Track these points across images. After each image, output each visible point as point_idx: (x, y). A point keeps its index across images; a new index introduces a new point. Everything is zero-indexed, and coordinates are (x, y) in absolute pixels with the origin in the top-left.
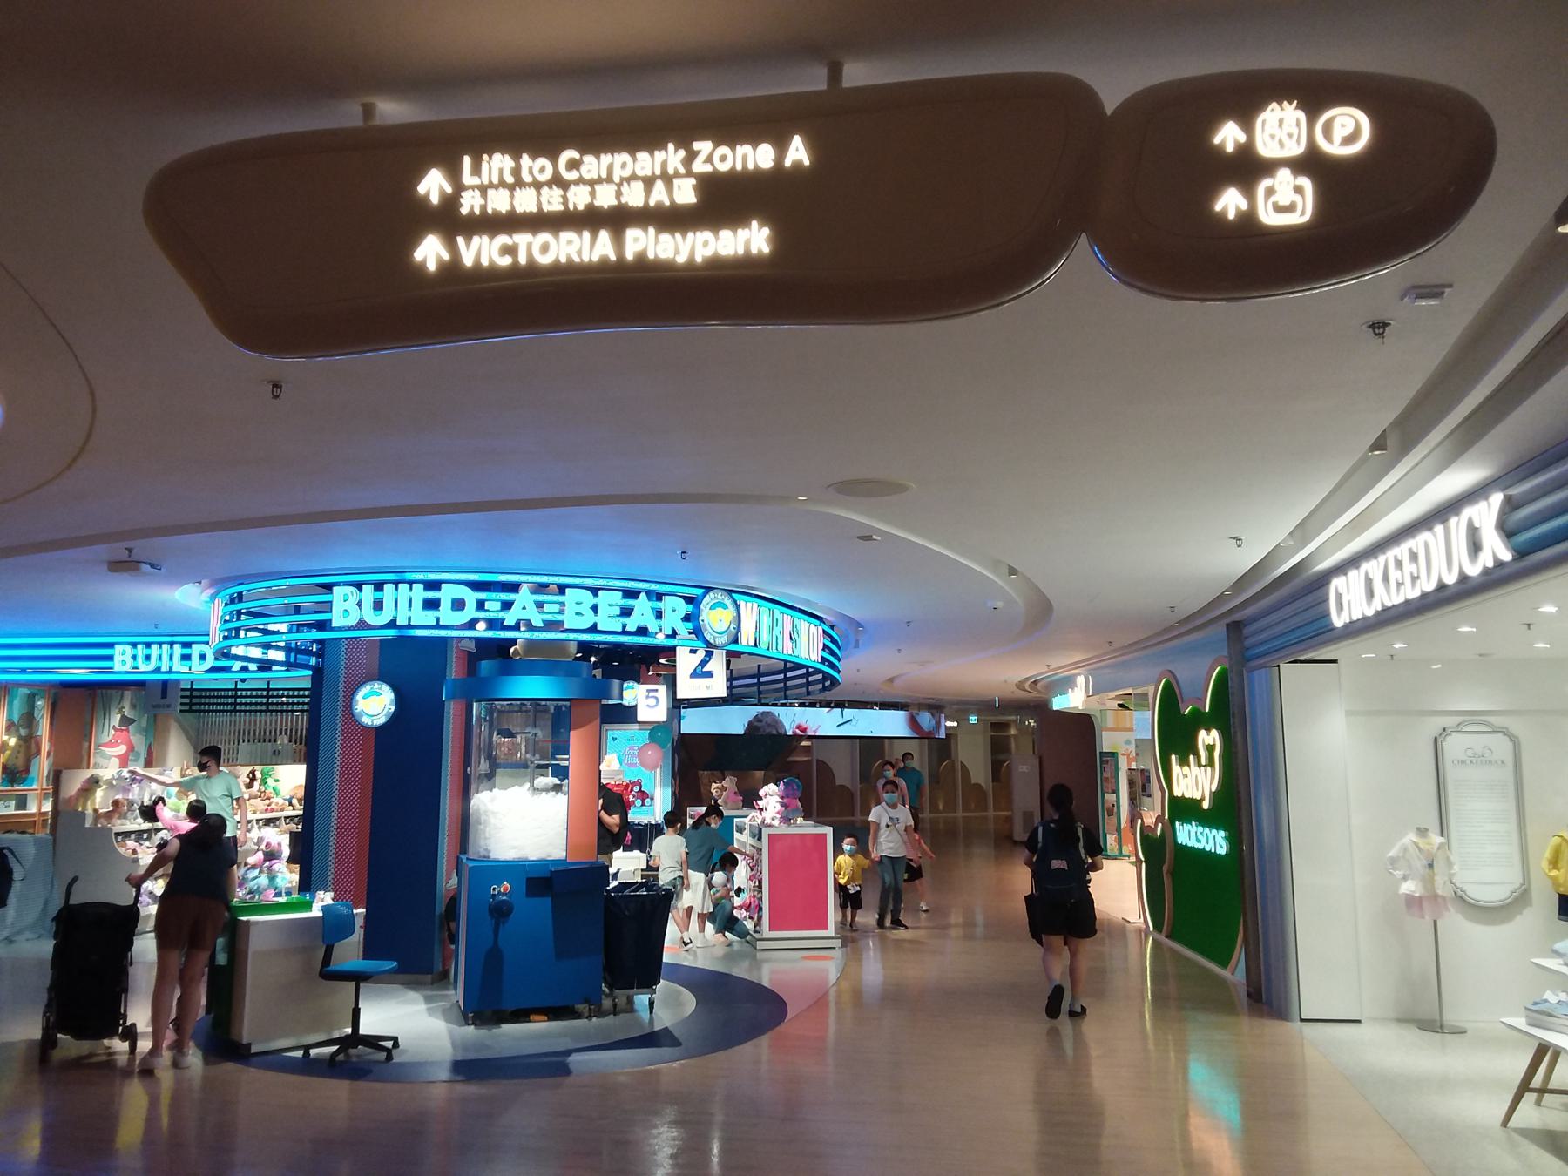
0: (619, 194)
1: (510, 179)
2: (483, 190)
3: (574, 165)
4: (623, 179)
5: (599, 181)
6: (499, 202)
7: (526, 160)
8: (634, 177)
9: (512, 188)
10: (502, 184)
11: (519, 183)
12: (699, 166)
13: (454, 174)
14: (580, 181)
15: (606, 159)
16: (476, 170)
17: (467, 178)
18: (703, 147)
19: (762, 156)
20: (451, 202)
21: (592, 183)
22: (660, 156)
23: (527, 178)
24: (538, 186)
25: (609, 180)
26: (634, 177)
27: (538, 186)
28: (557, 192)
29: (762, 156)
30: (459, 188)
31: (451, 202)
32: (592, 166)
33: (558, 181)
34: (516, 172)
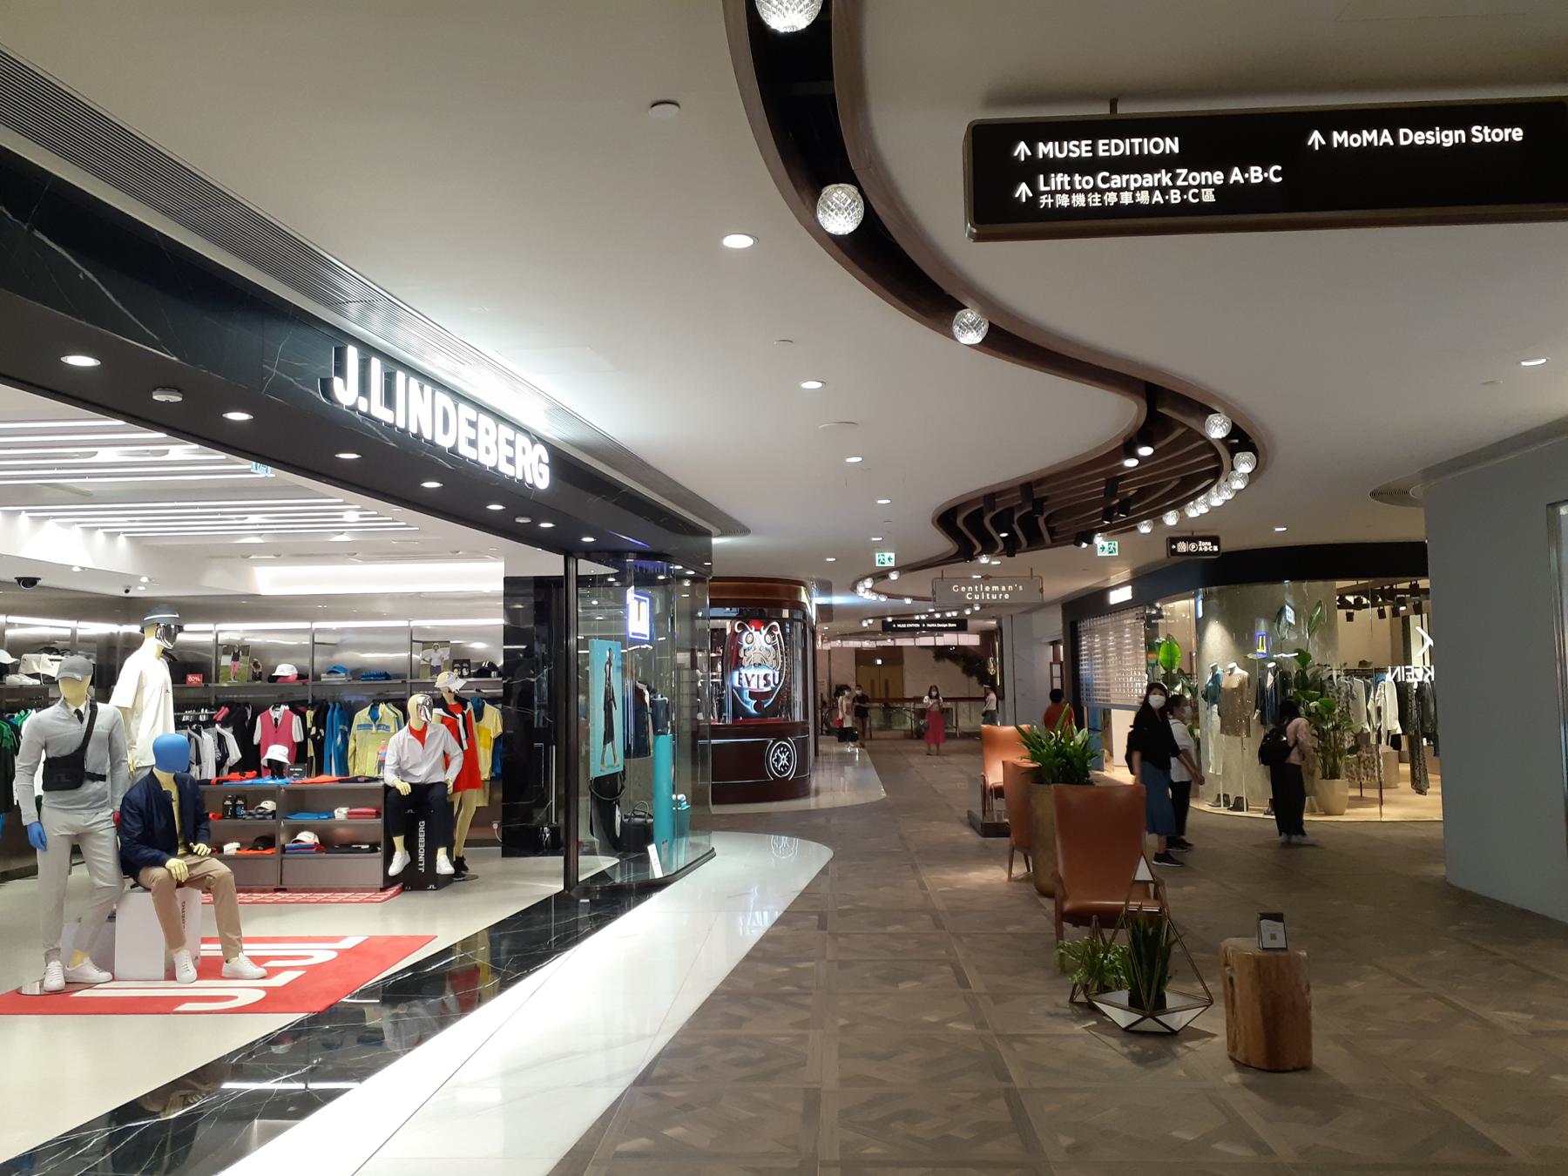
0: (1134, 198)
1: (1067, 188)
2: (1053, 194)
3: (1105, 180)
4: (1136, 189)
6: (1063, 200)
7: (1077, 178)
8: (1141, 188)
9: (1070, 193)
10: (1062, 191)
11: (1072, 191)
12: (1180, 183)
13: (1033, 186)
14: (1110, 190)
15: (1125, 177)
16: (1046, 184)
17: (1042, 188)
18: (1185, 171)
19: (1218, 178)
20: (1034, 200)
21: (1118, 191)
22: (1157, 176)
23: (1078, 187)
25: (1127, 189)
26: (1141, 188)
28: (1097, 195)
30: (1037, 193)
31: (1034, 200)
32: (1117, 181)
33: (1095, 189)
34: (1071, 183)
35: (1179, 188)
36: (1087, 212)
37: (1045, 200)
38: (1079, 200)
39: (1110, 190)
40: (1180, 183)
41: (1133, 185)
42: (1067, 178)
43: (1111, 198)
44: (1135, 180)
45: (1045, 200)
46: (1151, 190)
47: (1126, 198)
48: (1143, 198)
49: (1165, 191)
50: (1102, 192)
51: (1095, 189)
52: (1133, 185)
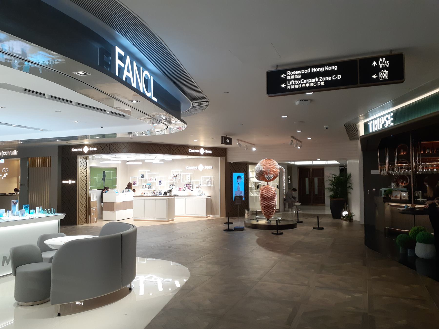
2: (290, 85)
3: (302, 81)
5: (306, 83)
6: (293, 87)
7: (296, 81)
9: (294, 85)
11: (295, 84)
12: (320, 80)
14: (304, 83)
17: (288, 84)
19: (329, 78)
21: (305, 83)
24: (298, 84)
25: (308, 83)
27: (298, 84)
29: (329, 78)
34: (295, 83)
35: (320, 82)
36: (298, 89)
37: (289, 87)
38: (296, 86)
39: (304, 83)
40: (320, 80)
41: (309, 82)
42: (294, 81)
43: (304, 85)
44: (310, 80)
45: (289, 87)
46: (313, 83)
47: (307, 85)
48: (311, 85)
49: (317, 82)
50: (302, 84)
51: (300, 83)
52: (309, 82)
